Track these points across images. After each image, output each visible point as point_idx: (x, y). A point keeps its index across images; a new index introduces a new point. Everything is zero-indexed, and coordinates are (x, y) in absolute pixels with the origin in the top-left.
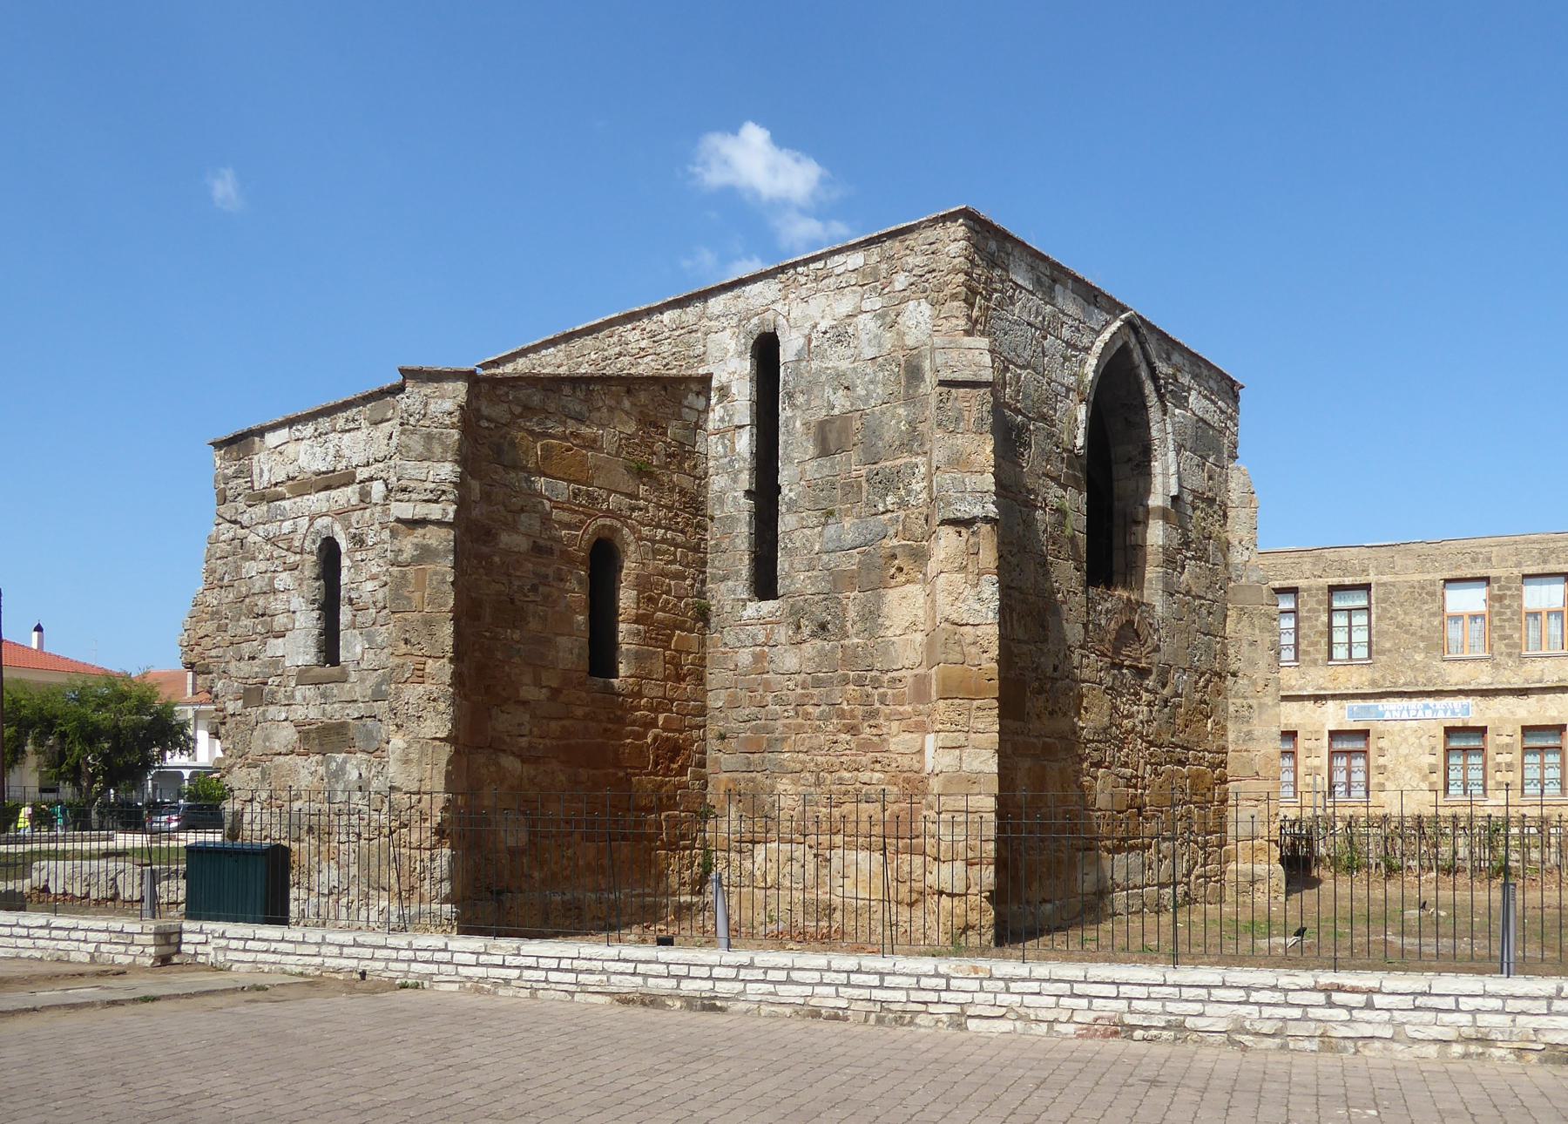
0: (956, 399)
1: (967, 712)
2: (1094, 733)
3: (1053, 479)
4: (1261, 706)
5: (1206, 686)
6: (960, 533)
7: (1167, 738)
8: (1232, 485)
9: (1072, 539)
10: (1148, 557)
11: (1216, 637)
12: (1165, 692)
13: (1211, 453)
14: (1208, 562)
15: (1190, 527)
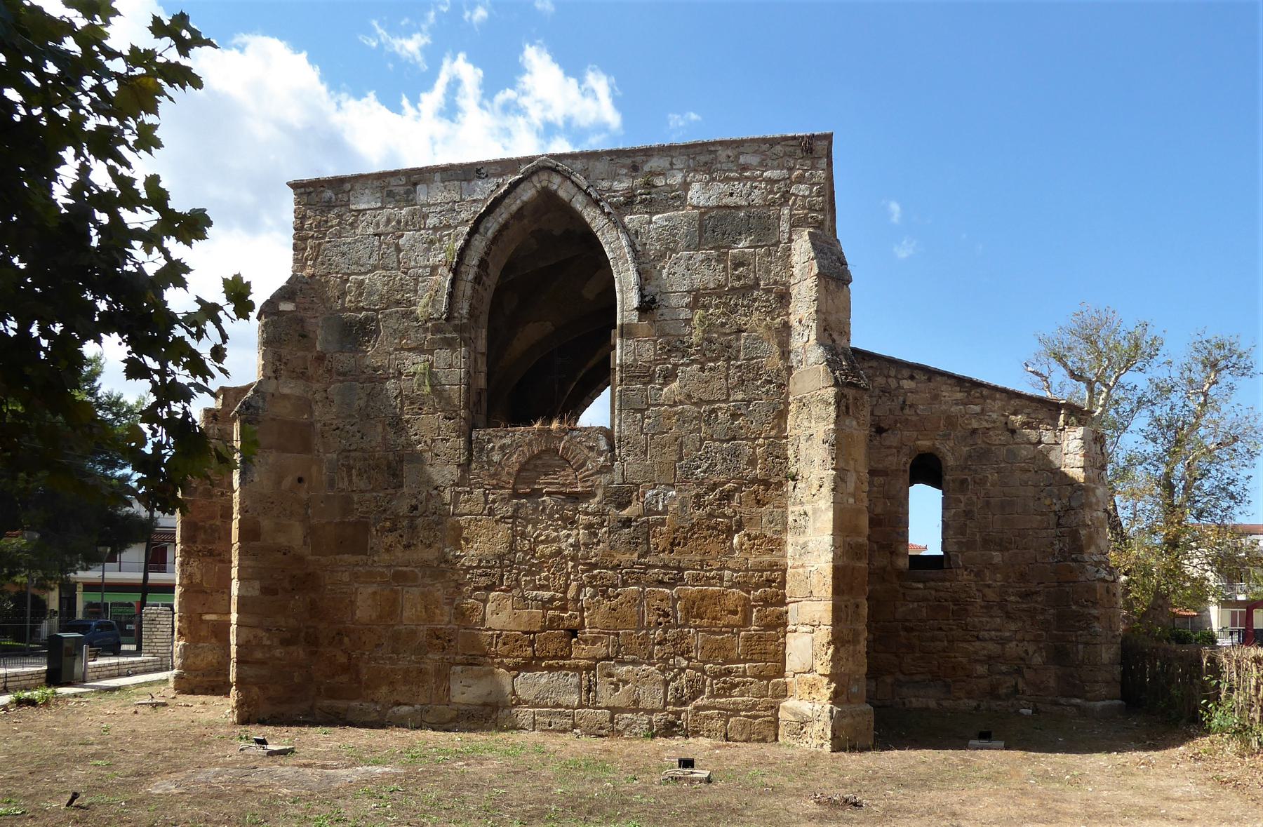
2: (480, 561)
3: (409, 350)
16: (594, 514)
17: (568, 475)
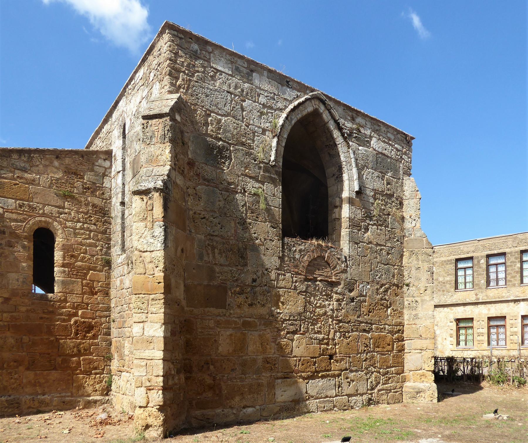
0: (151, 126)
1: (146, 302)
3: (251, 177)
4: (422, 301)
5: (386, 291)
6: (142, 199)
7: (353, 318)
8: (405, 188)
9: (268, 210)
10: (343, 224)
11: (394, 266)
12: (352, 294)
13: (389, 171)
14: (388, 227)
15: (372, 208)
16: (340, 294)
17: (328, 272)
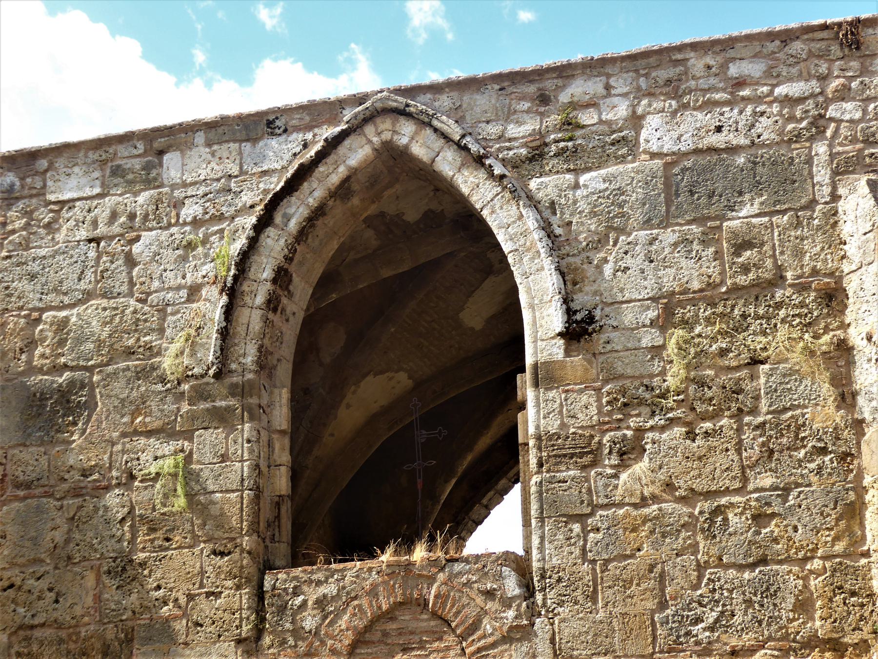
3: (149, 434)
